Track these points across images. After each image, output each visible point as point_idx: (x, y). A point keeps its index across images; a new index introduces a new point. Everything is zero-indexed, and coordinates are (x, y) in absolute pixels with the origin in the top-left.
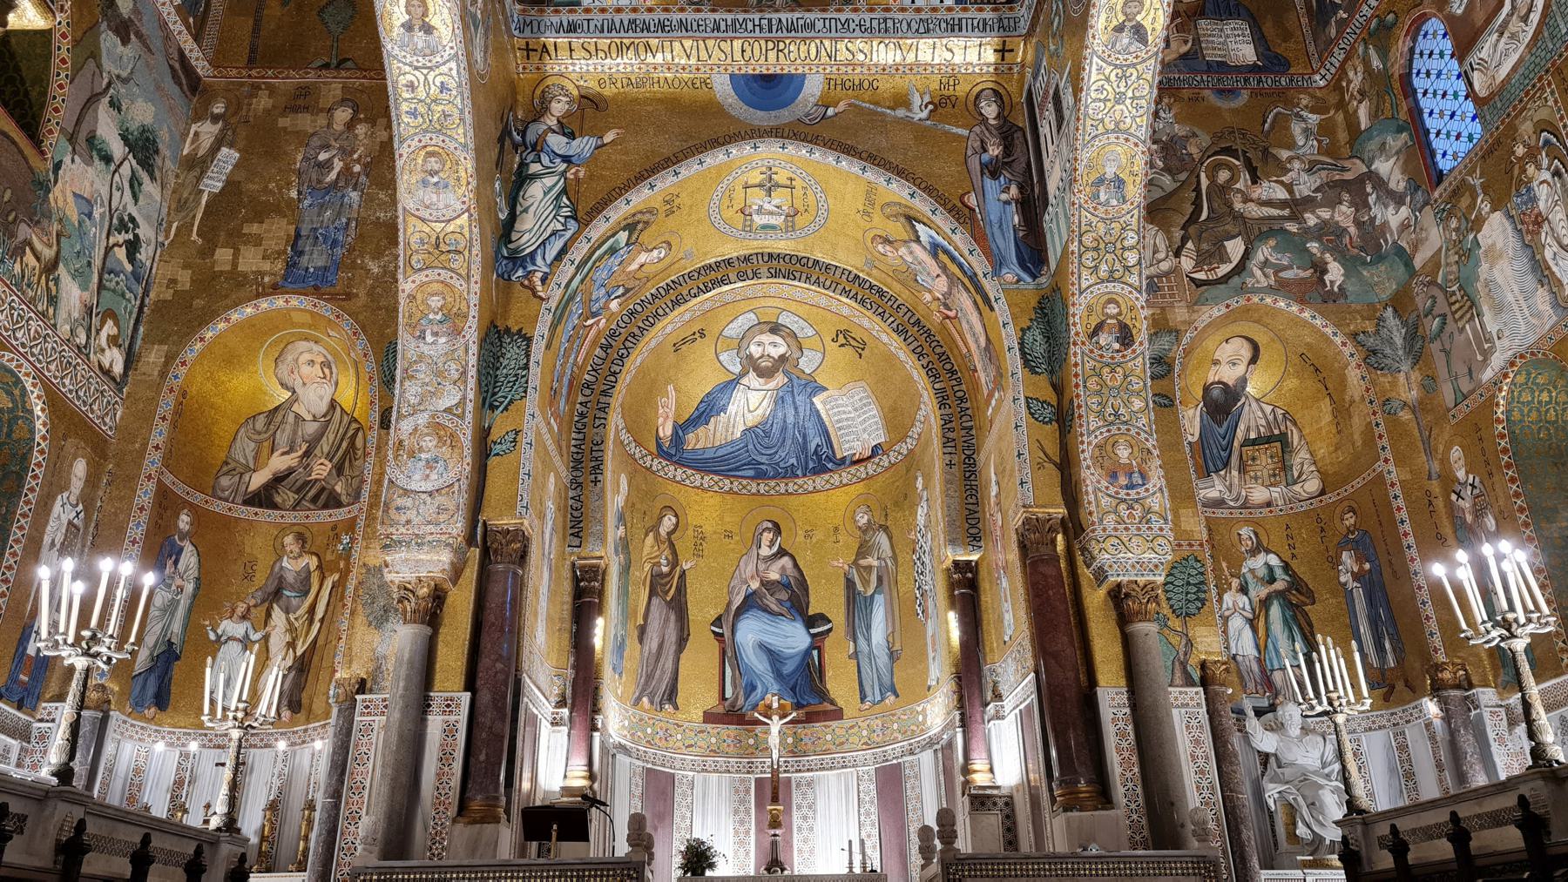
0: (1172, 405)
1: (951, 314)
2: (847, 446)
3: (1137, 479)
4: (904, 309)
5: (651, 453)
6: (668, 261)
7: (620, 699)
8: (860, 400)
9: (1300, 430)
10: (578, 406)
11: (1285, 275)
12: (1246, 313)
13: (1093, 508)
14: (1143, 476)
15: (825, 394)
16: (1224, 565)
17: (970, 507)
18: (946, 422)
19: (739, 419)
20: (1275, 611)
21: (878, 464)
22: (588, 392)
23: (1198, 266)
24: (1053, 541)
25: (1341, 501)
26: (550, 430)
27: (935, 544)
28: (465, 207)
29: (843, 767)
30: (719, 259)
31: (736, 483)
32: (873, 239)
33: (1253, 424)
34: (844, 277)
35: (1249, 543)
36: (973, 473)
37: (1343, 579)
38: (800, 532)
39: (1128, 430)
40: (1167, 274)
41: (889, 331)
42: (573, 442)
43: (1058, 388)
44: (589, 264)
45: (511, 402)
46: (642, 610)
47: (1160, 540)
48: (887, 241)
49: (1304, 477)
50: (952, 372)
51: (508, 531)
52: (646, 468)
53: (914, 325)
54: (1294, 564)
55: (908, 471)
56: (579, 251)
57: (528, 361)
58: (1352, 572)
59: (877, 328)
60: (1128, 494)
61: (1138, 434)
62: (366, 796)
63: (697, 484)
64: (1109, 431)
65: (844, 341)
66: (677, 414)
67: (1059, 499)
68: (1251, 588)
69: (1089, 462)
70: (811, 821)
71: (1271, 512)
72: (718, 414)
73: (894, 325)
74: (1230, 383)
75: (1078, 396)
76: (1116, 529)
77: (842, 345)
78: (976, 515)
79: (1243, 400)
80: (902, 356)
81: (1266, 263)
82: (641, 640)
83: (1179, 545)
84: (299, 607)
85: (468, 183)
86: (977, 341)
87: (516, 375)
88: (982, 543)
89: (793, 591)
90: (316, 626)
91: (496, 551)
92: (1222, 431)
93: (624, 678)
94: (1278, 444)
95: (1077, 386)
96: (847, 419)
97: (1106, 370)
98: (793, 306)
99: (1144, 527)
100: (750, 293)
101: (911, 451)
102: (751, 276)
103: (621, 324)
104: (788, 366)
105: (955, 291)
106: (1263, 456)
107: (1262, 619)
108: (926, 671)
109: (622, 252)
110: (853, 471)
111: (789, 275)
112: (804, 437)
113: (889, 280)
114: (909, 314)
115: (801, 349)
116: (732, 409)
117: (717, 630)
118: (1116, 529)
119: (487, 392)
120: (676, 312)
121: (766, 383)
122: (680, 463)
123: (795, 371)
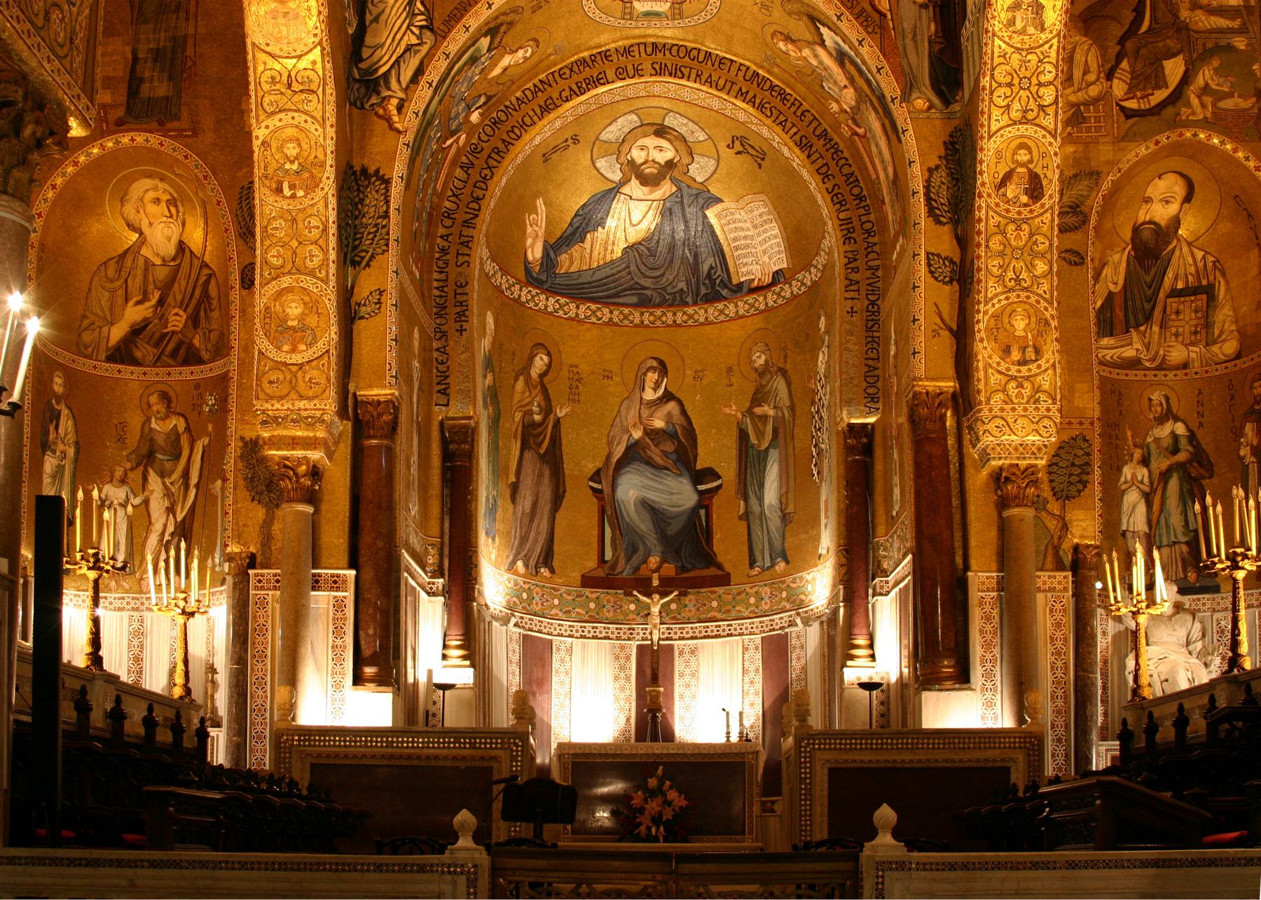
0: (1082, 263)
1: (861, 131)
2: (744, 270)
3: (1030, 354)
4: (809, 117)
5: (519, 281)
6: (535, 58)
7: (496, 565)
8: (761, 215)
9: (1227, 283)
10: (439, 240)
11: (1227, 104)
12: (1177, 149)
13: (981, 386)
14: (1038, 351)
15: (719, 207)
16: (1129, 434)
17: (870, 362)
18: (851, 260)
19: (620, 235)
20: (1174, 484)
21: (779, 294)
22: (448, 222)
23: (1130, 94)
24: (943, 417)
25: (1254, 367)
26: (413, 281)
27: (833, 399)
28: (317, 40)
29: (729, 635)
30: (595, 51)
31: (616, 313)
32: (773, 35)
33: (1182, 271)
34: (741, 74)
35: (1159, 409)
36: (876, 322)
37: (1242, 453)
38: (689, 372)
39: (1028, 297)
40: (1095, 101)
41: (792, 144)
42: (435, 284)
43: (964, 241)
44: (448, 81)
45: (372, 257)
46: (513, 466)
47: (1046, 422)
48: (788, 39)
49: (1224, 337)
50: (860, 198)
51: (379, 402)
52: (514, 299)
53: (819, 137)
54: (1200, 434)
55: (811, 306)
56: (434, 74)
57: (388, 207)
58: (1252, 445)
59: (777, 139)
60: (1019, 371)
61: (1038, 302)
62: (269, 664)
63: (572, 314)
64: (1007, 298)
65: (741, 149)
66: (548, 233)
67: (951, 371)
68: (1153, 459)
69: (983, 334)
70: (693, 689)
71: (1186, 374)
72: (595, 230)
73: (797, 138)
74: (1163, 223)
75: (979, 257)
76: (1002, 410)
77: (739, 153)
78: (876, 372)
79: (1175, 242)
80: (805, 174)
81: (1206, 89)
82: (513, 499)
83: (1070, 423)
84: (172, 472)
85: (320, 13)
86: (885, 170)
87: (376, 225)
88: (880, 405)
89: (679, 442)
90: (193, 492)
91: (368, 422)
92: (1148, 279)
93: (497, 539)
94: (1204, 297)
95: (979, 245)
96: (745, 238)
97: (1011, 227)
98: (682, 108)
99: (1031, 407)
100: (630, 93)
101: (814, 283)
102: (631, 73)
103: (485, 138)
104: (676, 174)
105: (863, 107)
106: (1188, 310)
107: (1159, 493)
108: (817, 539)
109: (483, 59)
110: (751, 301)
111: (676, 72)
112: (696, 256)
113: (792, 81)
114: (815, 123)
115: (691, 154)
116: (611, 223)
117: (595, 485)
118: (1002, 410)
119: (347, 246)
120: (545, 121)
121: (651, 192)
122: (552, 291)
123: (684, 178)
